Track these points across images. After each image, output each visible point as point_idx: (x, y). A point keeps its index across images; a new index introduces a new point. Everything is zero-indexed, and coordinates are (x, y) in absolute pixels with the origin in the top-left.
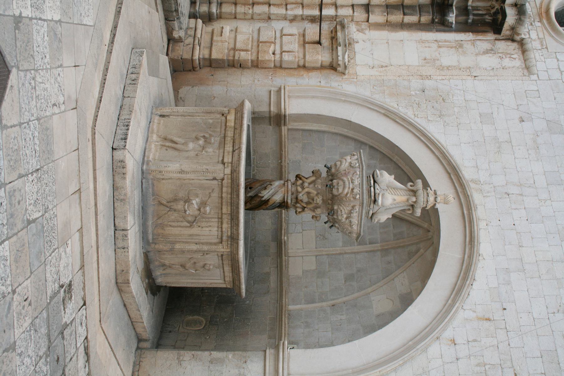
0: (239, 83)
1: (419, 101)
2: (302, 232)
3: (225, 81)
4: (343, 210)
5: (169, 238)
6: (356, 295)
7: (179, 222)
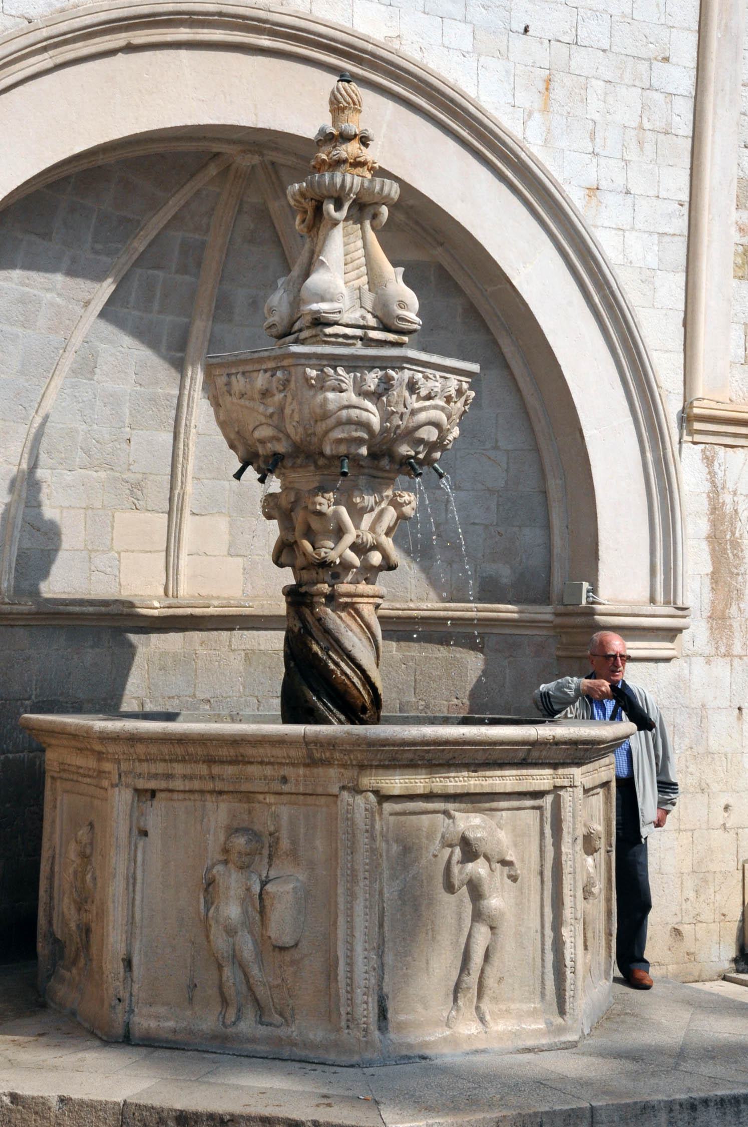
2: (119, 553)
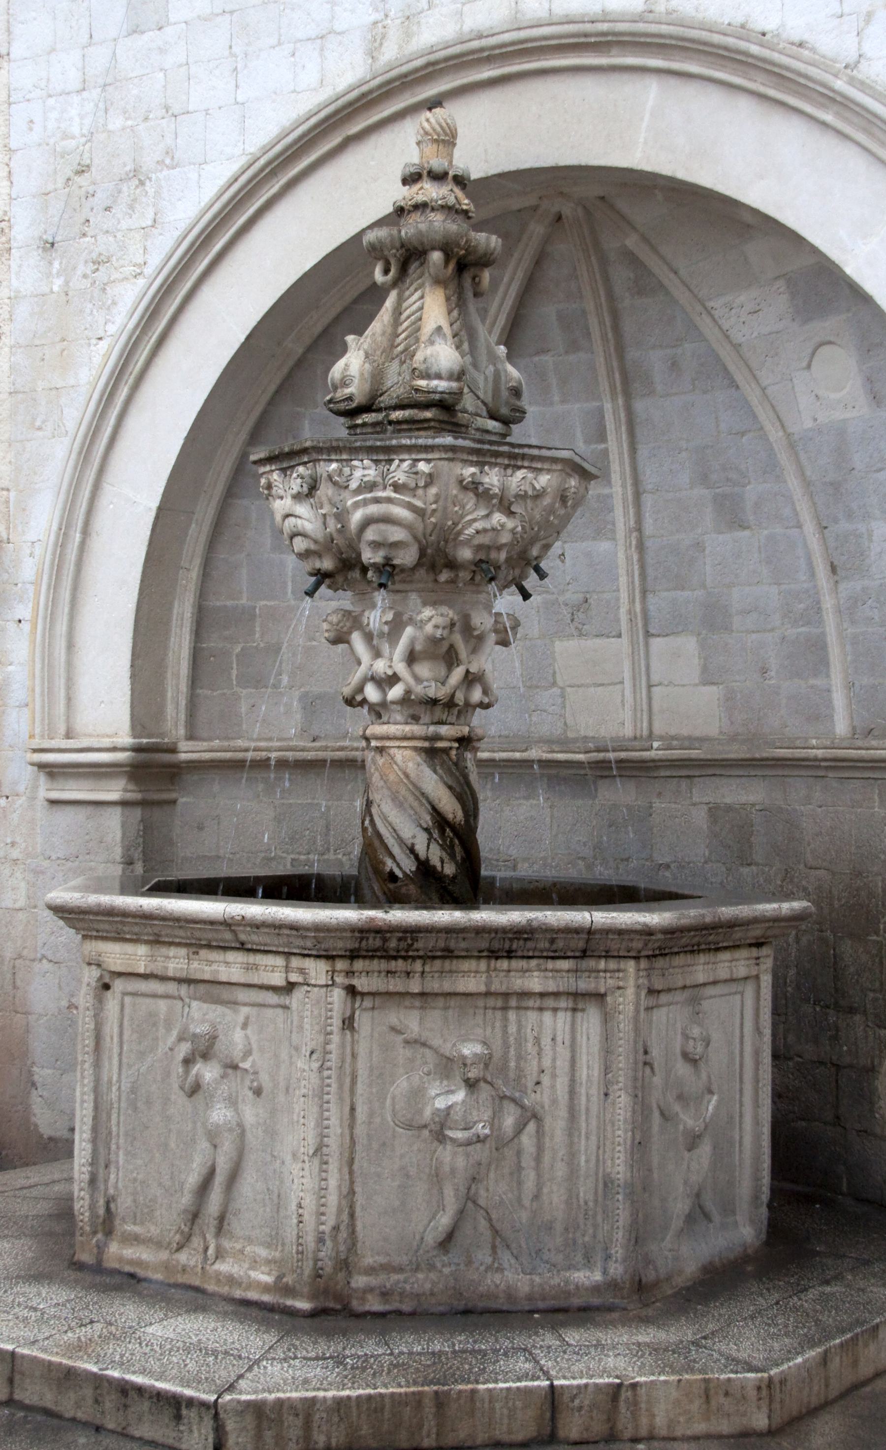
0: (21, 916)
1: (86, 262)
3: (14, 967)
4: (479, 525)
5: (586, 1203)
6: (794, 484)
7: (519, 1162)
